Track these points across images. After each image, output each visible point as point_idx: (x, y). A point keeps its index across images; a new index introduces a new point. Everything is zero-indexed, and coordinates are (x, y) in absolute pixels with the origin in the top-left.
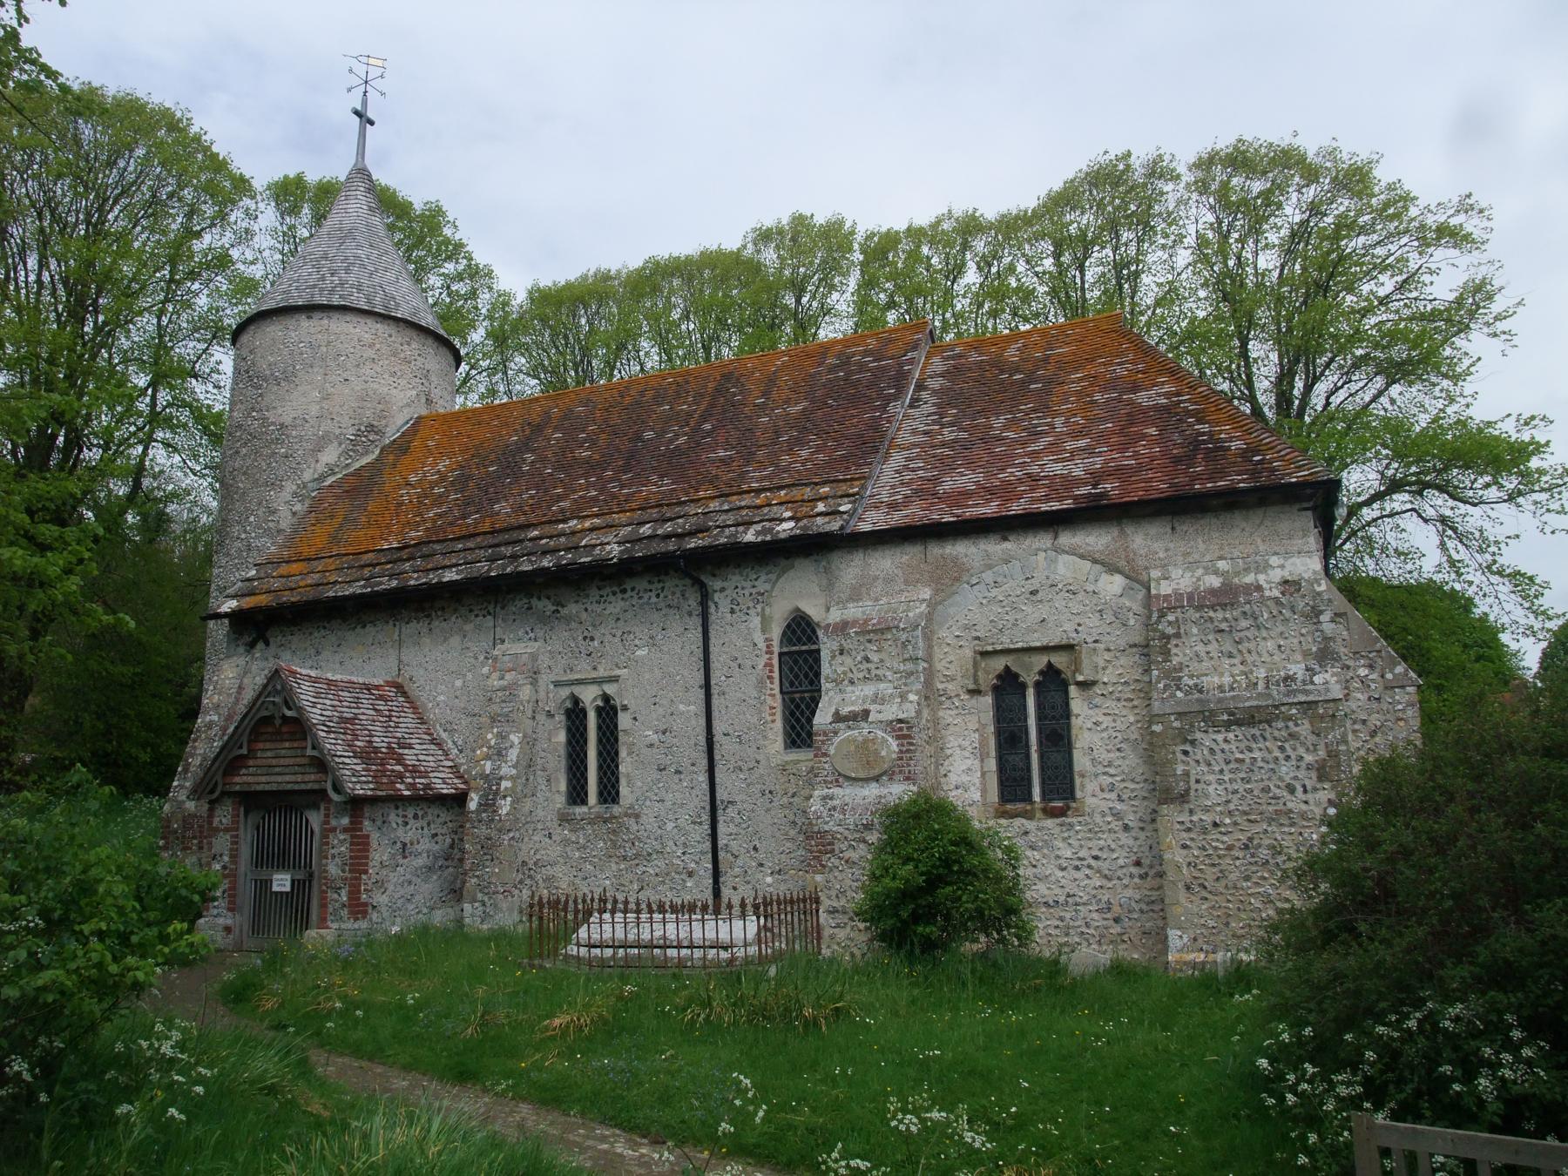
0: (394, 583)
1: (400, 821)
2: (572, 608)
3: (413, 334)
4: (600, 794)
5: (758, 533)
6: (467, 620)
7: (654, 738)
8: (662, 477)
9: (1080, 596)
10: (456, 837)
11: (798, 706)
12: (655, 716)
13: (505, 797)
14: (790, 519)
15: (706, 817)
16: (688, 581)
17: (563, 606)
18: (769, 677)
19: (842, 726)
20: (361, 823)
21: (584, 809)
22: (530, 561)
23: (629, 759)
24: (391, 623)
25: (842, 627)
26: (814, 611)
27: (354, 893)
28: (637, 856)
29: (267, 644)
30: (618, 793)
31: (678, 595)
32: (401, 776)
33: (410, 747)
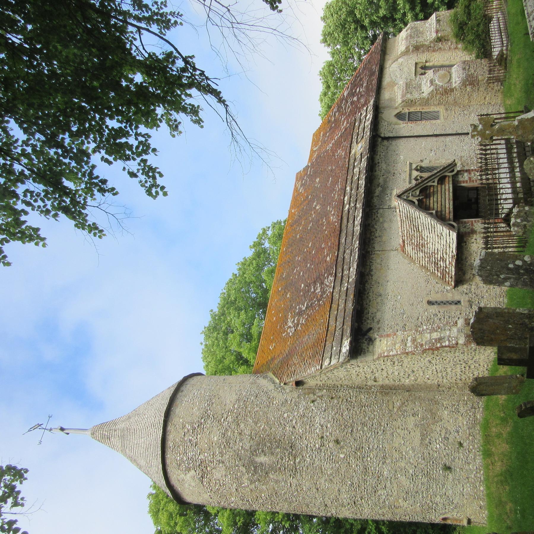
6: (378, 220)
17: (380, 184)
31: (383, 147)
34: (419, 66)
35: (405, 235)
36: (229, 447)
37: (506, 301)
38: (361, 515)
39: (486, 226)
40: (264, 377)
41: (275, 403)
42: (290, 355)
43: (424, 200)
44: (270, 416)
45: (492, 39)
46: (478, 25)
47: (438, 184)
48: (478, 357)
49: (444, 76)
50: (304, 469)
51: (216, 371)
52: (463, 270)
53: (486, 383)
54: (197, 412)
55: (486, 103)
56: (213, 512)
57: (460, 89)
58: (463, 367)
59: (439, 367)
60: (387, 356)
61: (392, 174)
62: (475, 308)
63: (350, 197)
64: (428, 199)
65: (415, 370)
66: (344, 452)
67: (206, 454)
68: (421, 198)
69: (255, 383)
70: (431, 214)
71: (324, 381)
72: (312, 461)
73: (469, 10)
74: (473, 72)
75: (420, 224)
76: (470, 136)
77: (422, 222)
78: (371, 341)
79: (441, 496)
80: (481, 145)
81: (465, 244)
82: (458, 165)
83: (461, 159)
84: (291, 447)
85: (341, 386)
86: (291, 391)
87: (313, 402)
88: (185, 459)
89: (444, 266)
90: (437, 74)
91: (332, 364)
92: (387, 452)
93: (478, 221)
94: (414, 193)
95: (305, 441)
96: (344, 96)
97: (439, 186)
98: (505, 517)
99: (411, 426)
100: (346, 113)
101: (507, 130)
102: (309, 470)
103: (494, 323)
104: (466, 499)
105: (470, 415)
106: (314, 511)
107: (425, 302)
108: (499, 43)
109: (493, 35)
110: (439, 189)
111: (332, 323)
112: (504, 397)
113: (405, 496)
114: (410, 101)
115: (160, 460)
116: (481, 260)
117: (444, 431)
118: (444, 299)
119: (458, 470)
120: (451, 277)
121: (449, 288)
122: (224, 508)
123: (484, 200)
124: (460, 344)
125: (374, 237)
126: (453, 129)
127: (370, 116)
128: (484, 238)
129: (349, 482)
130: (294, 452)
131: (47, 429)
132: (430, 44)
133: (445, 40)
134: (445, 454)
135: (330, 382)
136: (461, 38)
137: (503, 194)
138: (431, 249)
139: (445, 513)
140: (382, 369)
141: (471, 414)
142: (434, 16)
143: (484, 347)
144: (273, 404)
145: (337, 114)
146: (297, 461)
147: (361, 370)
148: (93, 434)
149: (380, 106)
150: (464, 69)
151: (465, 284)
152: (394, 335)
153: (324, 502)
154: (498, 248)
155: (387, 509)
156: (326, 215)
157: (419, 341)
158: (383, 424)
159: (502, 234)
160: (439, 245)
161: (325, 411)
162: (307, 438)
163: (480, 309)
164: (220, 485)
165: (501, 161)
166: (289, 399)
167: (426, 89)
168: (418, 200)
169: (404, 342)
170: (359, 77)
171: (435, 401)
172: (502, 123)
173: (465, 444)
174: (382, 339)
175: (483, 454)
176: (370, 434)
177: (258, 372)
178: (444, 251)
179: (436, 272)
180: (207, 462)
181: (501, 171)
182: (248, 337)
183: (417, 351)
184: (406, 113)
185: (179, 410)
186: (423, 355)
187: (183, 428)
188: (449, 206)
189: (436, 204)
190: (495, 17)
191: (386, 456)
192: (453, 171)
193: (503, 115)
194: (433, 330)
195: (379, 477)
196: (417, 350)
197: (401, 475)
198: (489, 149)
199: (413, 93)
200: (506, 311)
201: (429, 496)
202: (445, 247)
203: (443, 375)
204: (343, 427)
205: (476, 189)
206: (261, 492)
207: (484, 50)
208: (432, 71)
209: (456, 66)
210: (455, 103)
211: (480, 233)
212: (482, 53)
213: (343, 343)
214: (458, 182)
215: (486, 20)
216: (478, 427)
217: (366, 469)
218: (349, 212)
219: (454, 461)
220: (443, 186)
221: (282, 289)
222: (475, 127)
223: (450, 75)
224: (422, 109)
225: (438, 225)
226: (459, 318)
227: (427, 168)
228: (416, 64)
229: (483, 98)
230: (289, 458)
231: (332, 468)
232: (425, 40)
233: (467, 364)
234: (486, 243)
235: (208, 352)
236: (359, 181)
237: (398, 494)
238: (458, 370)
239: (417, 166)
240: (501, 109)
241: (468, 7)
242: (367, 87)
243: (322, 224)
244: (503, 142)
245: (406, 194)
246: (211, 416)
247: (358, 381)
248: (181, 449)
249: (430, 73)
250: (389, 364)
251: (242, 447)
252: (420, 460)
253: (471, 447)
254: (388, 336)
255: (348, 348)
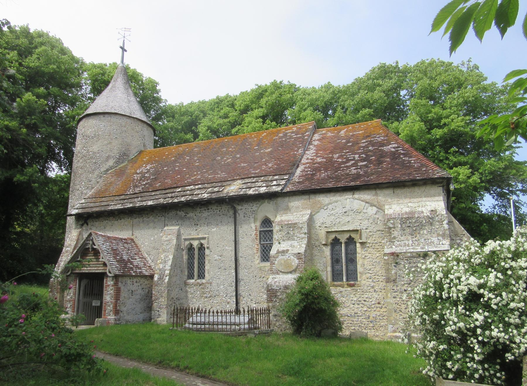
0: (131, 205)
1: (131, 283)
2: (191, 214)
3: (140, 123)
4: (199, 276)
5: (253, 191)
7: (217, 258)
8: (222, 172)
9: (361, 214)
10: (150, 289)
11: (265, 248)
12: (217, 250)
13: (167, 276)
14: (265, 186)
15: (234, 284)
16: (230, 206)
17: (188, 214)
18: (256, 239)
19: (280, 255)
20: (118, 283)
21: (193, 281)
22: (177, 199)
23: (208, 265)
24: (130, 219)
25: (280, 224)
27: (115, 306)
28: (210, 296)
29: (87, 224)
30: (204, 276)
31: (226, 210)
32: (132, 268)
33: (135, 259)
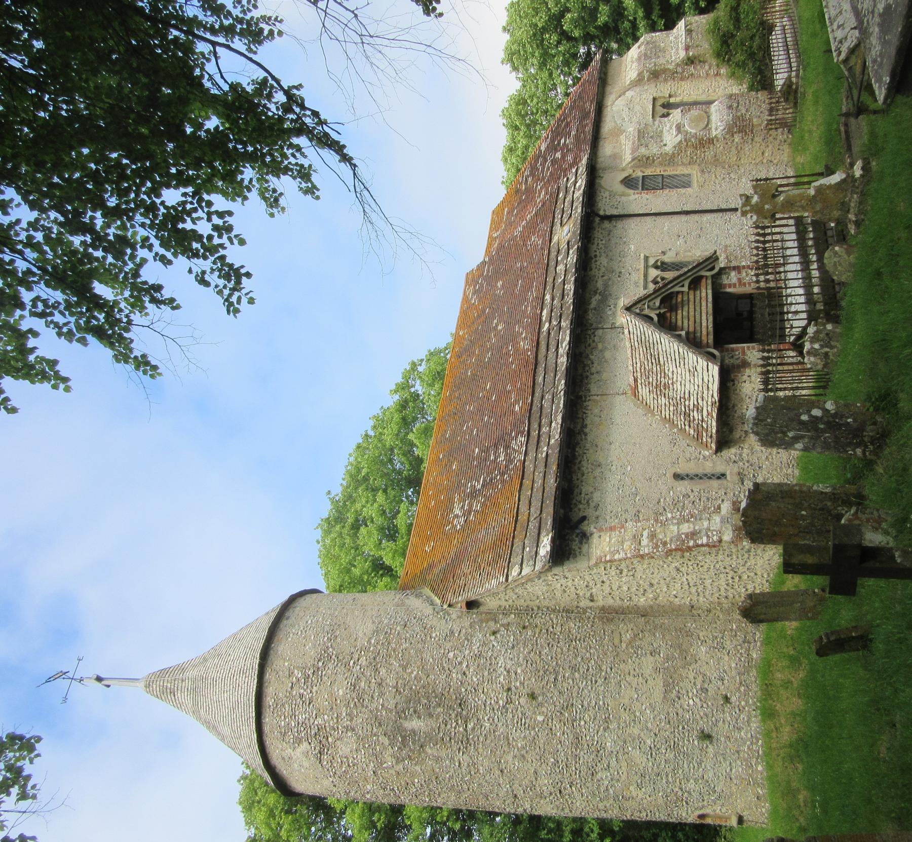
6: (596, 348)
17: (598, 289)
26: (624, 175)
31: (603, 232)
34: (659, 103)
35: (638, 369)
36: (363, 706)
37: (797, 472)
38: (571, 811)
39: (766, 354)
40: (416, 595)
41: (434, 635)
42: (458, 559)
43: (668, 315)
44: (427, 656)
45: (774, 60)
46: (752, 38)
47: (689, 288)
48: (753, 562)
49: (698, 119)
50: (481, 739)
51: (341, 586)
52: (729, 424)
53: (767, 602)
54: (311, 651)
55: (765, 161)
56: (338, 807)
57: (724, 138)
58: (729, 578)
59: (692, 578)
60: (610, 561)
61: (618, 274)
62: (749, 485)
63: (552, 311)
64: (674, 314)
65: (655, 582)
66: (543, 712)
67: (326, 717)
68: (662, 311)
69: (403, 604)
70: (679, 337)
71: (511, 601)
72: (493, 727)
73: (738, 14)
74: (744, 111)
75: (661, 352)
76: (739, 213)
77: (664, 350)
78: (585, 537)
79: (696, 781)
80: (757, 227)
81: (732, 383)
82: (722, 258)
83: (726, 251)
84: (460, 704)
85: (539, 608)
86: (459, 617)
87: (494, 633)
88: (293, 725)
89: (700, 418)
90: (688, 116)
91: (523, 573)
92: (610, 712)
93: (753, 348)
94: (651, 304)
95: (482, 695)
96: (540, 151)
97: (691, 292)
98: (796, 812)
99: (648, 670)
100: (543, 178)
101: (798, 204)
102: (488, 741)
103: (779, 508)
104: (736, 784)
105: (741, 654)
106: (497, 805)
107: (669, 475)
108: (785, 66)
109: (775, 54)
110: (691, 297)
111: (523, 508)
112: (795, 624)
113: (639, 781)
114: (644, 159)
115: (254, 727)
116: (757, 408)
117: (700, 679)
118: (700, 471)
119: (723, 739)
120: (711, 437)
121: (707, 453)
122: (355, 802)
123: (762, 314)
124: (726, 542)
125: (588, 374)
126: (712, 202)
127: (582, 183)
128: (762, 373)
129: (552, 760)
130: (464, 713)
131: (75, 679)
132: (676, 68)
133: (700, 61)
134: (702, 714)
135: (521, 602)
136: (724, 58)
137: (791, 304)
138: (679, 391)
139: (703, 807)
140: (603, 582)
141: (743, 651)
142: (681, 24)
143: (763, 546)
144: (431, 637)
145: (530, 179)
146: (470, 726)
147: (570, 583)
148: (148, 686)
149: (598, 166)
150: (730, 107)
151: (733, 446)
152: (621, 528)
153: (513, 791)
154: (785, 389)
155: (611, 801)
156: (514, 338)
157: (661, 537)
158: (604, 667)
159: (791, 367)
160: (692, 386)
161: (513, 647)
162: (486, 690)
163: (756, 485)
164: (349, 765)
165: (788, 252)
166: (456, 628)
167: (671, 139)
168: (658, 315)
169: (637, 539)
170: (564, 120)
171: (687, 632)
172: (789, 192)
173: (733, 699)
174: (602, 534)
175: (762, 714)
176: (584, 683)
177: (408, 587)
178: (700, 394)
179: (687, 427)
180: (328, 729)
181: (788, 267)
182: (390, 533)
183: (658, 553)
184: (639, 178)
185: (284, 648)
186: (667, 558)
187: (290, 676)
188: (706, 324)
189: (686, 322)
190: (778, 24)
191: (609, 718)
192: (713, 269)
193: (792, 180)
194: (684, 520)
195: (598, 751)
196: (658, 551)
197: (633, 748)
198: (769, 234)
199: (650, 146)
200: (797, 488)
201: (678, 780)
202: (701, 388)
203: (699, 590)
204: (542, 672)
205: (750, 297)
206: (413, 775)
207: (762, 76)
208: (679, 110)
209: (716, 102)
210: (716, 161)
211: (755, 366)
212: (758, 83)
213: (541, 540)
214: (722, 286)
215: (764, 29)
216: (754, 672)
217: (577, 738)
218: (549, 333)
219: (716, 725)
220: (698, 292)
221: (444, 456)
222: (748, 198)
223: (708, 117)
224: (664, 171)
225: (690, 354)
226: (723, 501)
227: (673, 264)
228: (654, 99)
229: (760, 153)
230: (456, 721)
231: (525, 737)
232: (668, 61)
233: (735, 572)
234: (766, 382)
235: (328, 557)
236: (564, 285)
237: (628, 777)
238: (722, 582)
239: (657, 261)
240: (789, 170)
241: (735, 9)
242: (577, 137)
243: (507, 354)
244: (791, 222)
245: (639, 305)
246: (333, 657)
247: (565, 601)
248: (287, 709)
249: (676, 114)
250: (614, 573)
251: (383, 705)
252: (663, 724)
253: (743, 703)
254: (612, 529)
255: (548, 548)
